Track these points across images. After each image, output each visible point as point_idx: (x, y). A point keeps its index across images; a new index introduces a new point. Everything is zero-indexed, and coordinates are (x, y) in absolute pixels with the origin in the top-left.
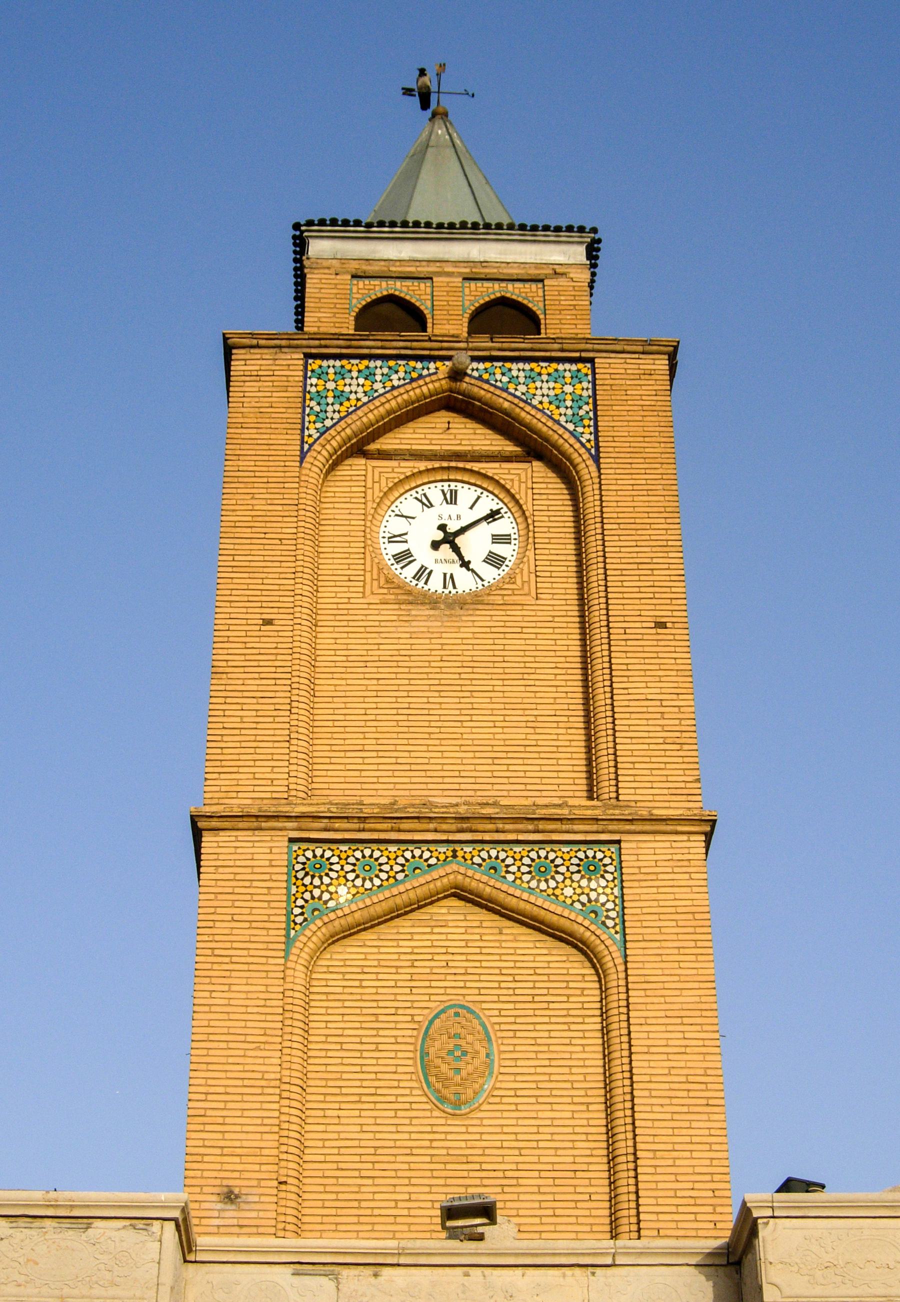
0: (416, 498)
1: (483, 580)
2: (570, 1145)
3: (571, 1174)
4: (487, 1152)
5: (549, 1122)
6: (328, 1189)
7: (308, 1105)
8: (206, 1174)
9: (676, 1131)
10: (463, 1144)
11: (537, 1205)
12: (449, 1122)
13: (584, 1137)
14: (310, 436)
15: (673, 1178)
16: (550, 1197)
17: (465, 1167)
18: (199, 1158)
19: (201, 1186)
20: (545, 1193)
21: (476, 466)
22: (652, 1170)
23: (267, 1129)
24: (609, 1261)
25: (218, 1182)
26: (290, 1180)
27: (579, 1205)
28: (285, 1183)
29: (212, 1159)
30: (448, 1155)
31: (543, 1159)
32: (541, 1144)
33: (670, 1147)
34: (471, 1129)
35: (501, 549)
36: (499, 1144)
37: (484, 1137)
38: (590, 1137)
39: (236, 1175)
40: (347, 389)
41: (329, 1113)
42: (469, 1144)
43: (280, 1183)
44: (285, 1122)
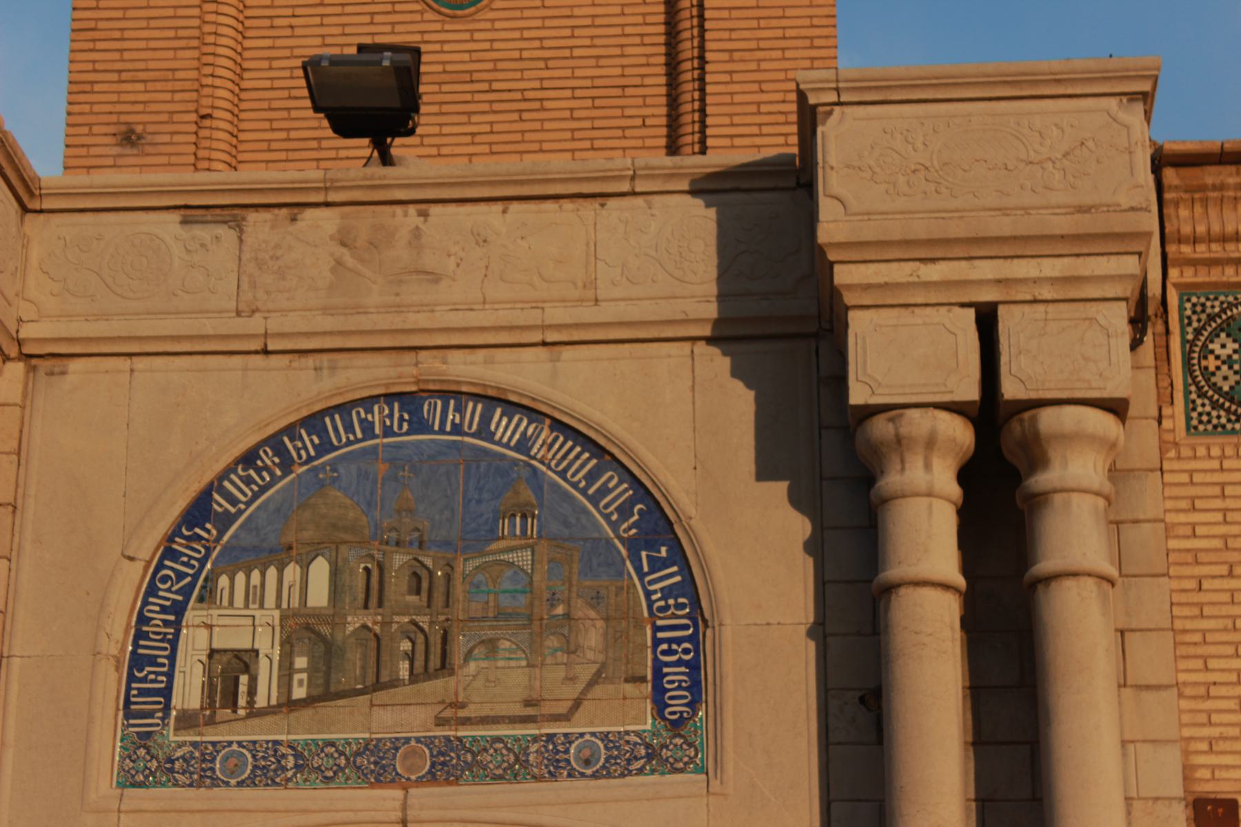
2: (617, 51)
3: (618, 92)
4: (500, 65)
5: (588, 21)
6: (276, 125)
7: (249, 13)
8: (96, 108)
9: (763, 23)
10: (466, 57)
11: (568, 135)
12: (447, 27)
13: (637, 40)
15: (755, 87)
16: (587, 124)
17: (467, 87)
18: (87, 87)
19: (90, 125)
20: (579, 119)
22: (726, 78)
23: (182, 43)
24: (625, 187)
25: (114, 118)
26: (217, 113)
27: (628, 133)
28: (209, 116)
29: (105, 87)
30: (445, 72)
31: (578, 73)
32: (577, 52)
33: (753, 45)
34: (477, 36)
36: (516, 54)
37: (497, 45)
38: (647, 40)
39: (140, 107)
41: (278, 22)
42: (475, 56)
43: (203, 117)
44: (210, 34)
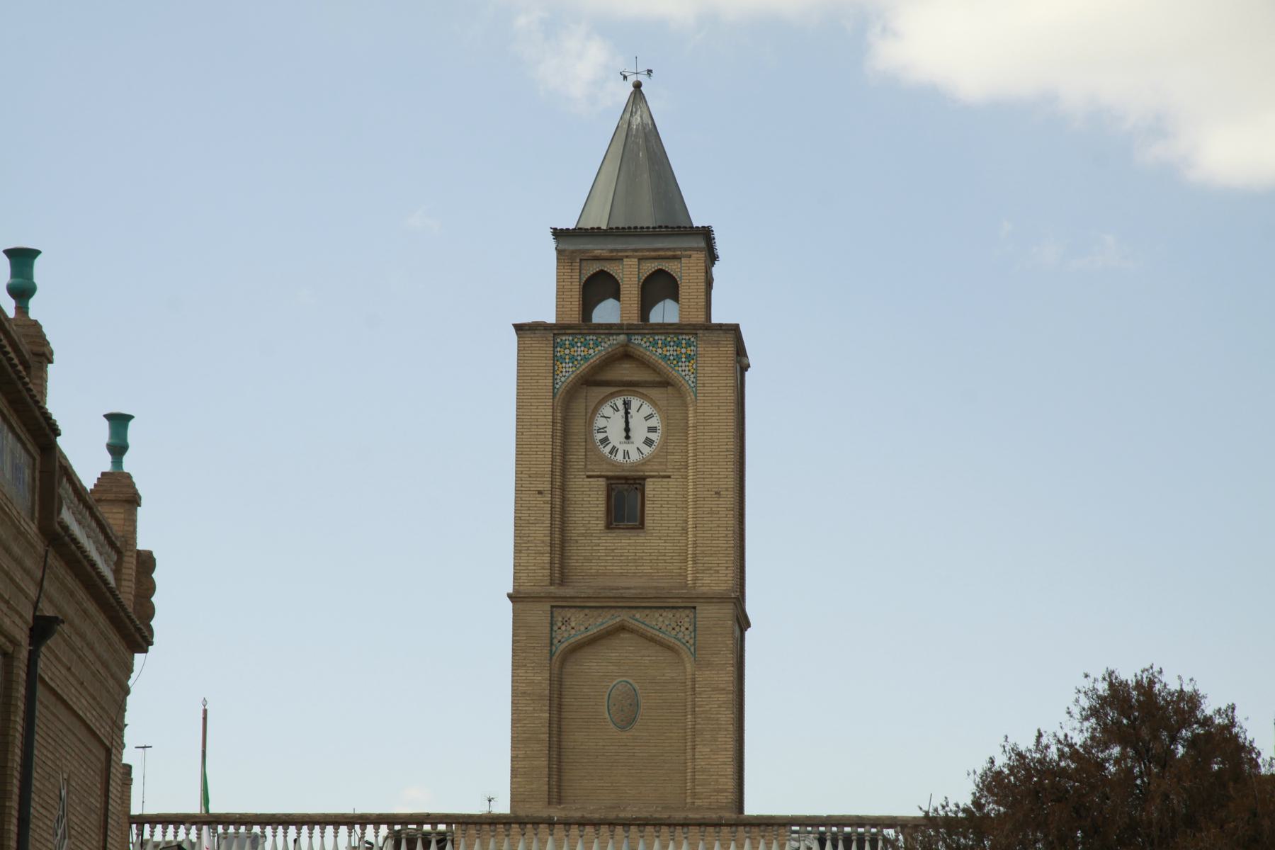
21: (640, 390)
35: (653, 436)
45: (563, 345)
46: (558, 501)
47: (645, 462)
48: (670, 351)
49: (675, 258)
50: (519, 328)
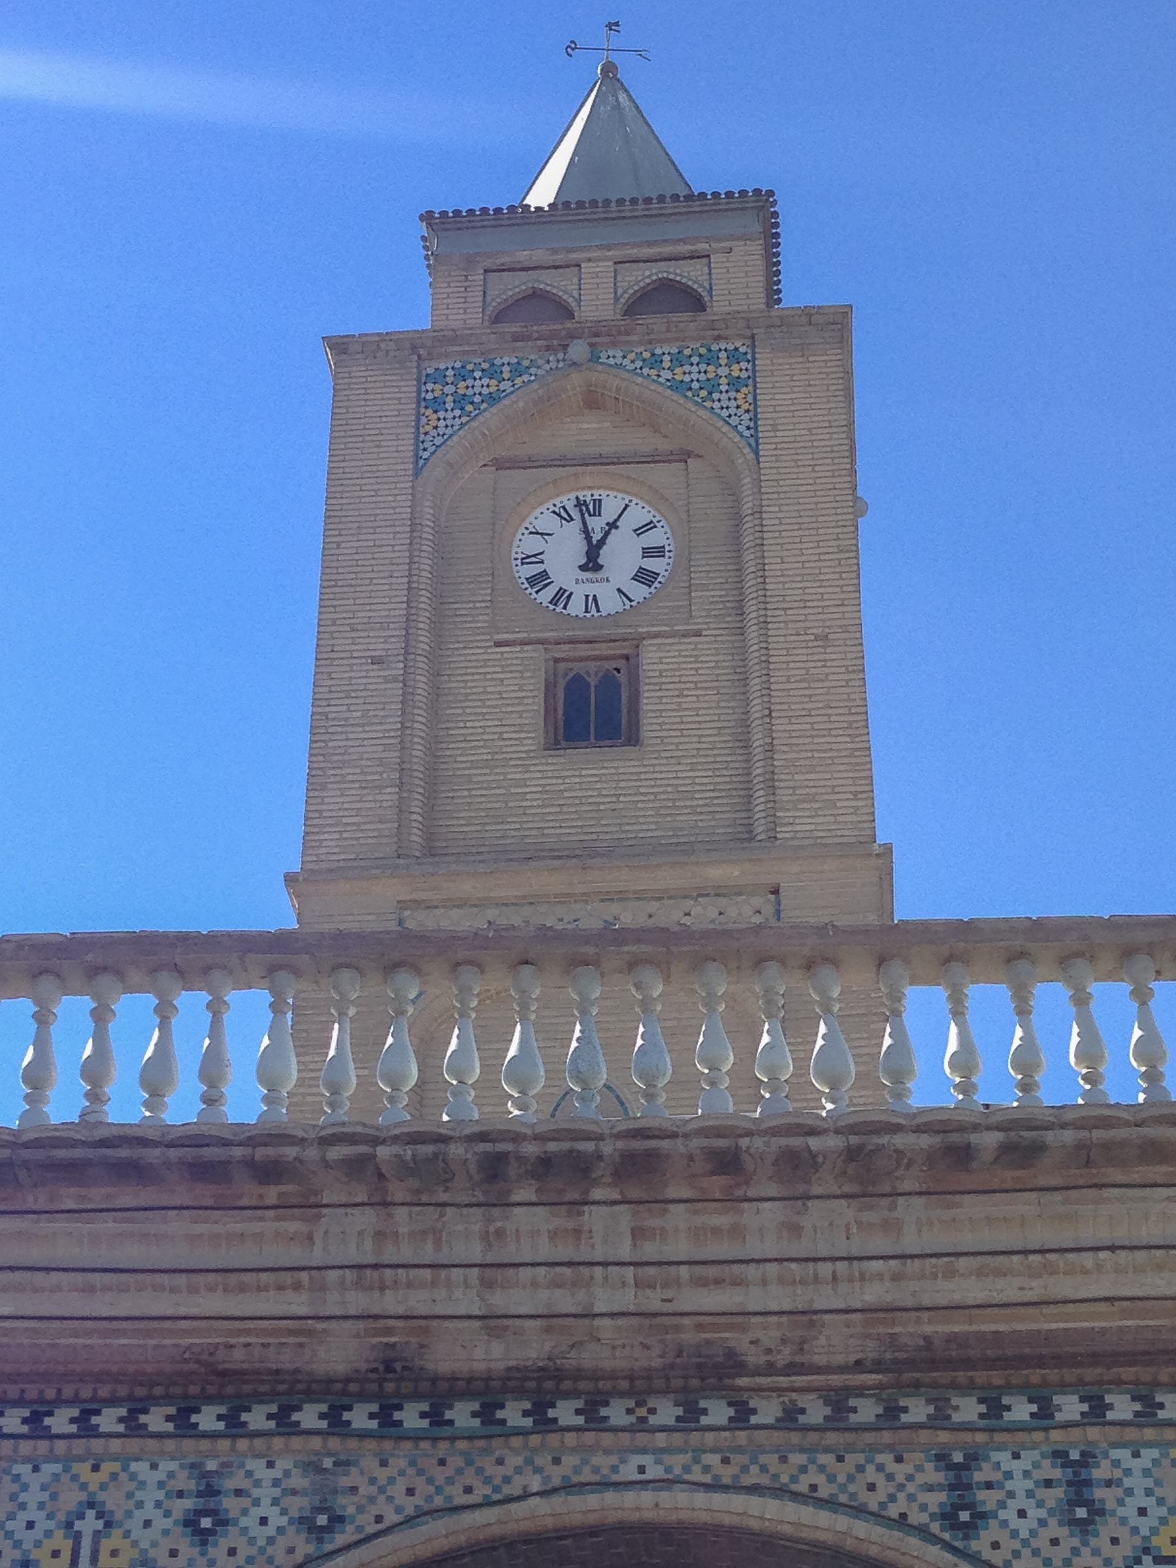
0: (554, 512)
1: (631, 601)
14: (425, 450)
35: (652, 564)
40: (470, 392)
45: (439, 377)
46: (421, 681)
47: (635, 609)
48: (692, 373)
49: (692, 257)
50: (339, 346)
